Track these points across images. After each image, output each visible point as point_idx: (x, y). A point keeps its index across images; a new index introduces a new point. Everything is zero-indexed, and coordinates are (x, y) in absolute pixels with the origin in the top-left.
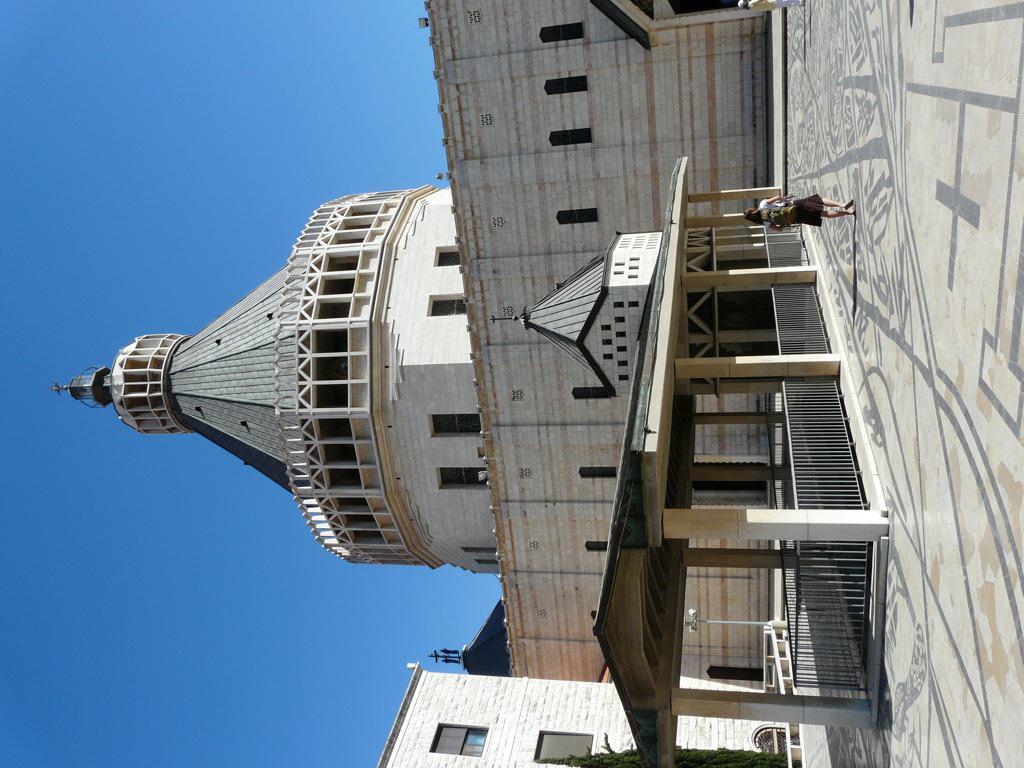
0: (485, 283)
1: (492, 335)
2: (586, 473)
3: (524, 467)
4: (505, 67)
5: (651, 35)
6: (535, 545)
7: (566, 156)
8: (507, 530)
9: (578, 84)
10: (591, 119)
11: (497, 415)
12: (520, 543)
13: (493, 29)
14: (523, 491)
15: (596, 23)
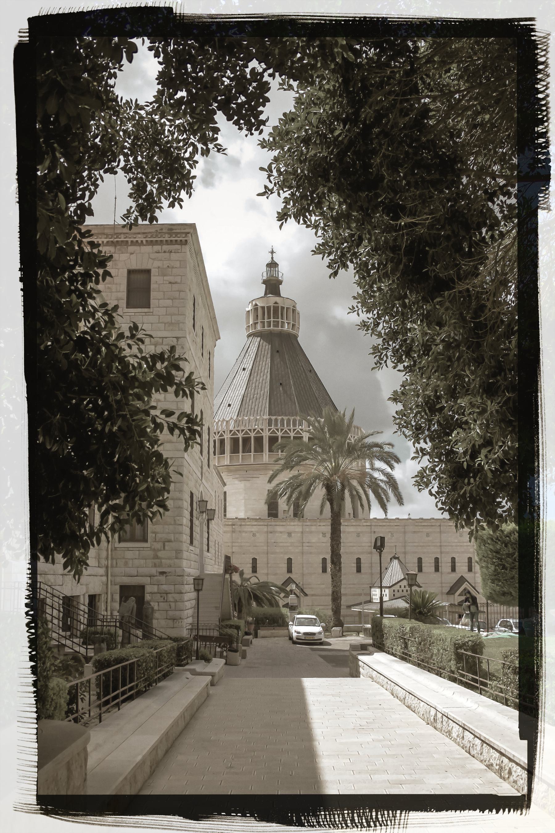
0: (369, 527)
1: (349, 527)
2: (290, 561)
3: (293, 535)
4: (445, 544)
5: (453, 596)
6: (254, 535)
7: (414, 563)
8: (262, 523)
9: (437, 569)
10: (425, 573)
11: (315, 525)
12: (254, 529)
13: (456, 541)
14: (281, 532)
15: (455, 577)
